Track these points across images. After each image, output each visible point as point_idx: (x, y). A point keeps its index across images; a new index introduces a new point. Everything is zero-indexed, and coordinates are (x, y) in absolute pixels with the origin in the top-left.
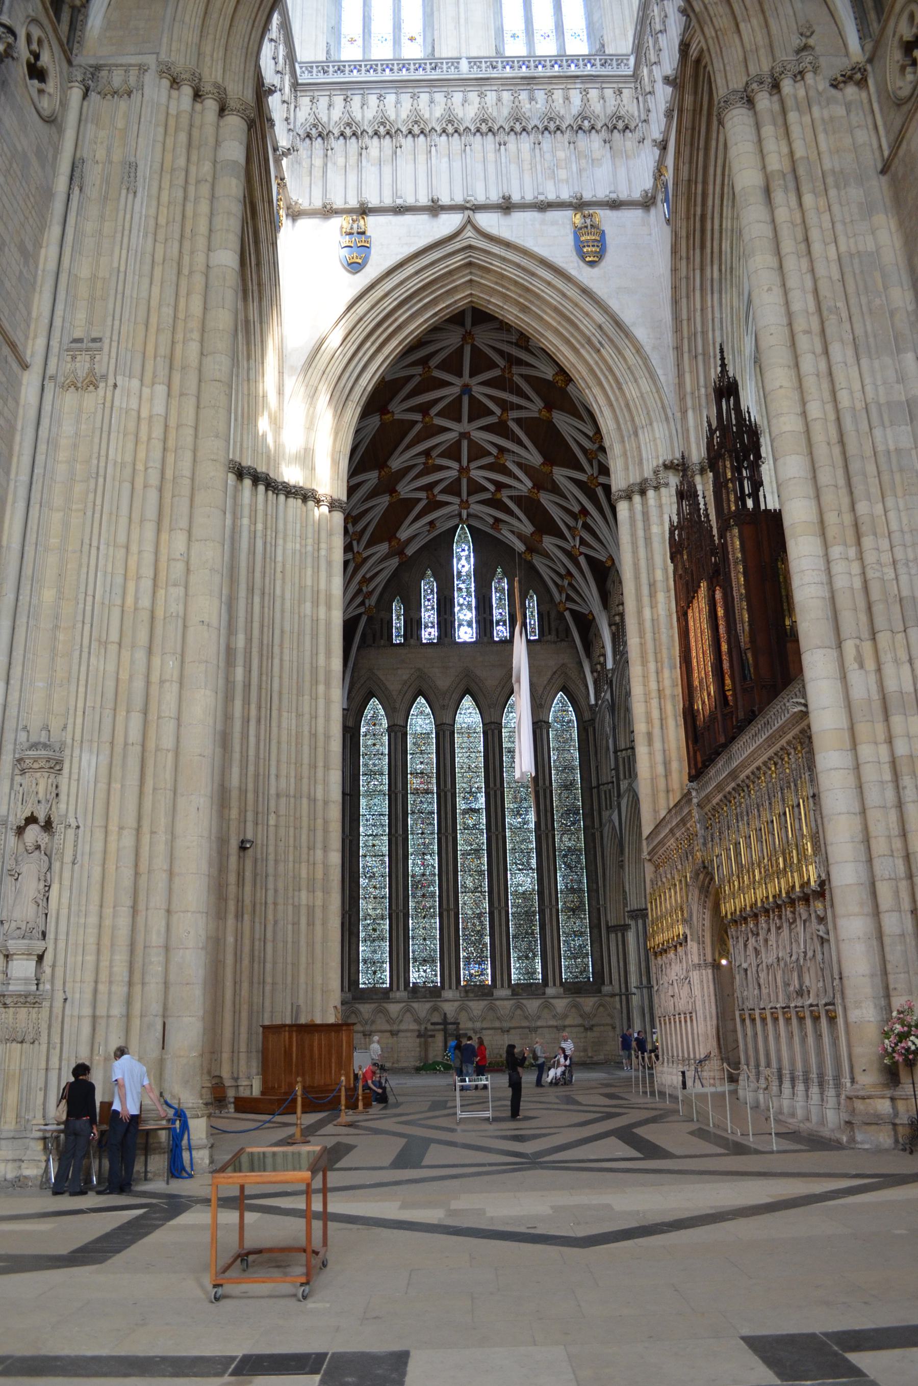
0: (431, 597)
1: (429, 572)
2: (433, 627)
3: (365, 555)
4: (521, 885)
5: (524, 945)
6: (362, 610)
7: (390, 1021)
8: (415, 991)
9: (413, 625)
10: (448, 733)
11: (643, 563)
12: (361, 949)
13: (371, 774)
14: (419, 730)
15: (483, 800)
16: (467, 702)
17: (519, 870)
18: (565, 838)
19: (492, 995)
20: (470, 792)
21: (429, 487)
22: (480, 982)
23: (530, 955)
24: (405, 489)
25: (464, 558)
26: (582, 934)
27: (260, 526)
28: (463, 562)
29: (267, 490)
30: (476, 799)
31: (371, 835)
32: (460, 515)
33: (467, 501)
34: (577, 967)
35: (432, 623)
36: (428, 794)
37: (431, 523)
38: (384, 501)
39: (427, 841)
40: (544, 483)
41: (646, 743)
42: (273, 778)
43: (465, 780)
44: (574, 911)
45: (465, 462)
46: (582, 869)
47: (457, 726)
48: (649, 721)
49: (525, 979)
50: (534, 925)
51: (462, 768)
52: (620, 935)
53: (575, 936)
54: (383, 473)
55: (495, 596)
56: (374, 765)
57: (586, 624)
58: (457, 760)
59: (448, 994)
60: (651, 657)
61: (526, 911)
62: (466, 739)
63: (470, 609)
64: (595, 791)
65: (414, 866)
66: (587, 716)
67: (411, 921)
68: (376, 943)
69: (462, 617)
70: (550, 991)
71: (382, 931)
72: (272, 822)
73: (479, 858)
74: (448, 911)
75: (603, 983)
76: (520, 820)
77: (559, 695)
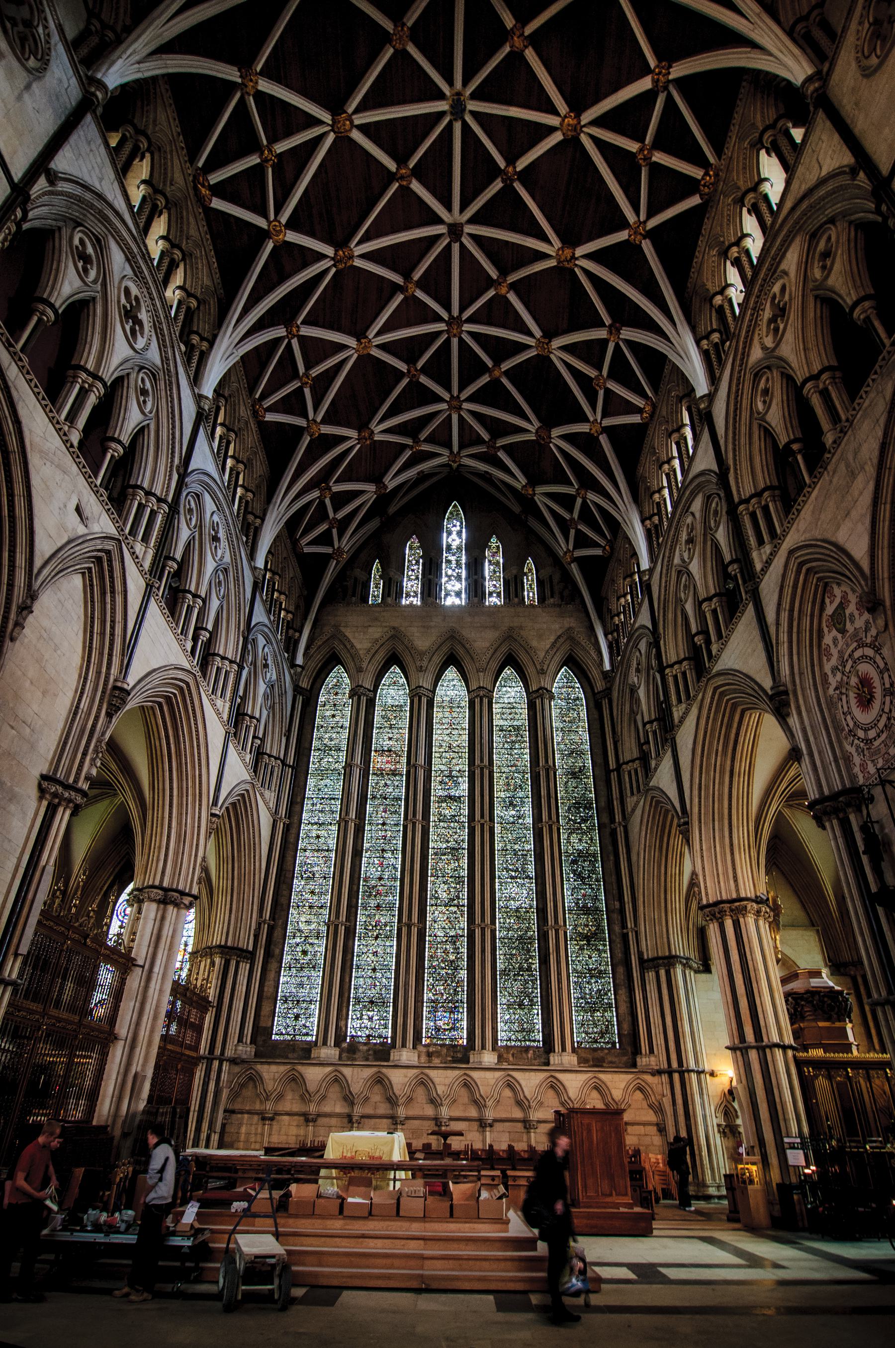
0: (415, 567)
2: (416, 596)
4: (514, 899)
5: (517, 986)
7: (305, 1096)
9: (393, 589)
10: (424, 700)
12: (282, 980)
13: (326, 750)
14: (390, 702)
15: (465, 786)
16: (451, 673)
17: (512, 878)
18: (574, 839)
19: (468, 1062)
20: (450, 776)
22: (452, 1040)
23: (526, 1002)
25: (454, 533)
26: (600, 974)
28: (454, 536)
30: (457, 784)
31: (316, 823)
33: (458, 397)
34: (595, 1025)
35: (415, 592)
36: (395, 775)
39: (389, 834)
43: (444, 761)
44: (589, 939)
46: (597, 880)
47: (437, 699)
49: (517, 1040)
50: (531, 957)
52: (662, 972)
53: (591, 977)
55: (487, 569)
56: (331, 739)
58: (435, 737)
61: (521, 936)
62: (447, 714)
64: (614, 776)
65: (370, 867)
66: (600, 685)
67: (357, 943)
68: (306, 972)
69: (449, 587)
71: (315, 955)
73: (458, 860)
74: (409, 927)
75: (637, 1051)
76: (514, 813)
77: (563, 670)
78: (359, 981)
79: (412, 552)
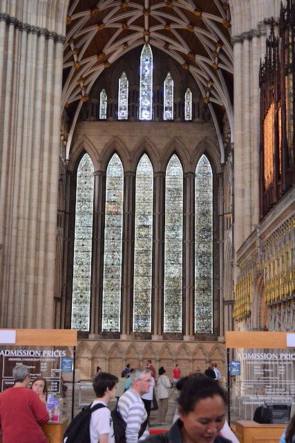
1: (124, 74)
3: (82, 63)
5: (172, 310)
6: (80, 97)
8: (106, 335)
9: (113, 108)
11: (246, 84)
13: (83, 201)
15: (152, 220)
16: (145, 158)
18: (201, 246)
19: (151, 339)
21: (124, 21)
23: (176, 316)
24: (108, 22)
27: (10, 52)
28: (146, 68)
29: (15, 28)
30: (147, 219)
32: (144, 38)
33: (148, 30)
37: (125, 44)
38: (95, 30)
39: (116, 244)
40: (196, 22)
41: (241, 196)
42: (15, 207)
45: (147, 6)
46: (210, 265)
48: (243, 182)
51: (139, 200)
54: (93, 12)
55: (165, 91)
57: (220, 112)
58: (136, 194)
59: (123, 337)
60: (247, 143)
62: (143, 182)
63: (149, 99)
64: (221, 218)
65: (107, 258)
67: (104, 292)
68: (82, 305)
69: (144, 104)
70: (186, 338)
72: (14, 234)
75: (219, 335)
78: (105, 308)
79: (123, 83)
